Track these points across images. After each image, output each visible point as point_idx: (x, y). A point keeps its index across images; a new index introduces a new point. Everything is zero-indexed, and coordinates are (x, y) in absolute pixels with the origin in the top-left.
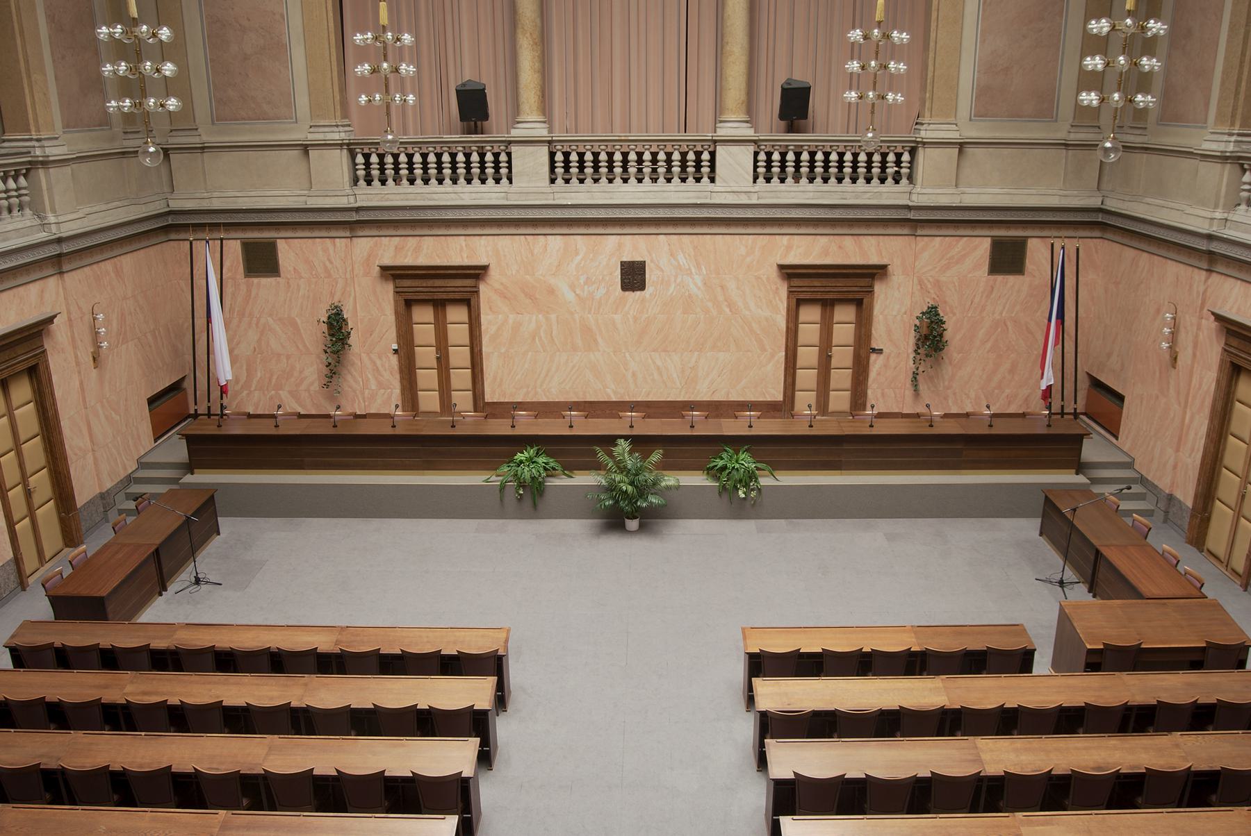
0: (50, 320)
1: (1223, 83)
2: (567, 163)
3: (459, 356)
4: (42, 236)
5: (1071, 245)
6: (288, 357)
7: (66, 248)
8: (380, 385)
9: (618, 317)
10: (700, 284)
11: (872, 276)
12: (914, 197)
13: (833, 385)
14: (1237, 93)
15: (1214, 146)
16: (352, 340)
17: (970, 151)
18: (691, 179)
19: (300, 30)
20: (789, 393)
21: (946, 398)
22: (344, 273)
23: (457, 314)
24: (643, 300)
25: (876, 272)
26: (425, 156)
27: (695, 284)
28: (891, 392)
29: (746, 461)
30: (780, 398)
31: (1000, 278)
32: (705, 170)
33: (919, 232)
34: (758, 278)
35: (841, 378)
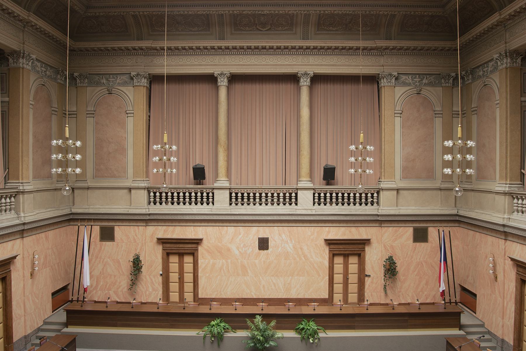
0: (15, 257)
1: (500, 164)
2: (236, 197)
3: (188, 277)
4: (17, 222)
5: (447, 230)
6: (115, 276)
7: (26, 227)
8: (154, 289)
9: (257, 261)
10: (292, 247)
11: (364, 244)
12: (380, 211)
13: (350, 291)
14: (506, 168)
15: (500, 189)
16: (143, 270)
17: (401, 192)
18: (287, 204)
19: (132, 143)
20: (331, 295)
21: (399, 296)
22: (142, 241)
23: (188, 259)
24: (268, 254)
25: (366, 242)
26: (178, 193)
27: (290, 248)
28: (375, 294)
29: (313, 325)
30: (327, 297)
31: (418, 244)
32: (293, 200)
33: (383, 225)
35: (353, 288)
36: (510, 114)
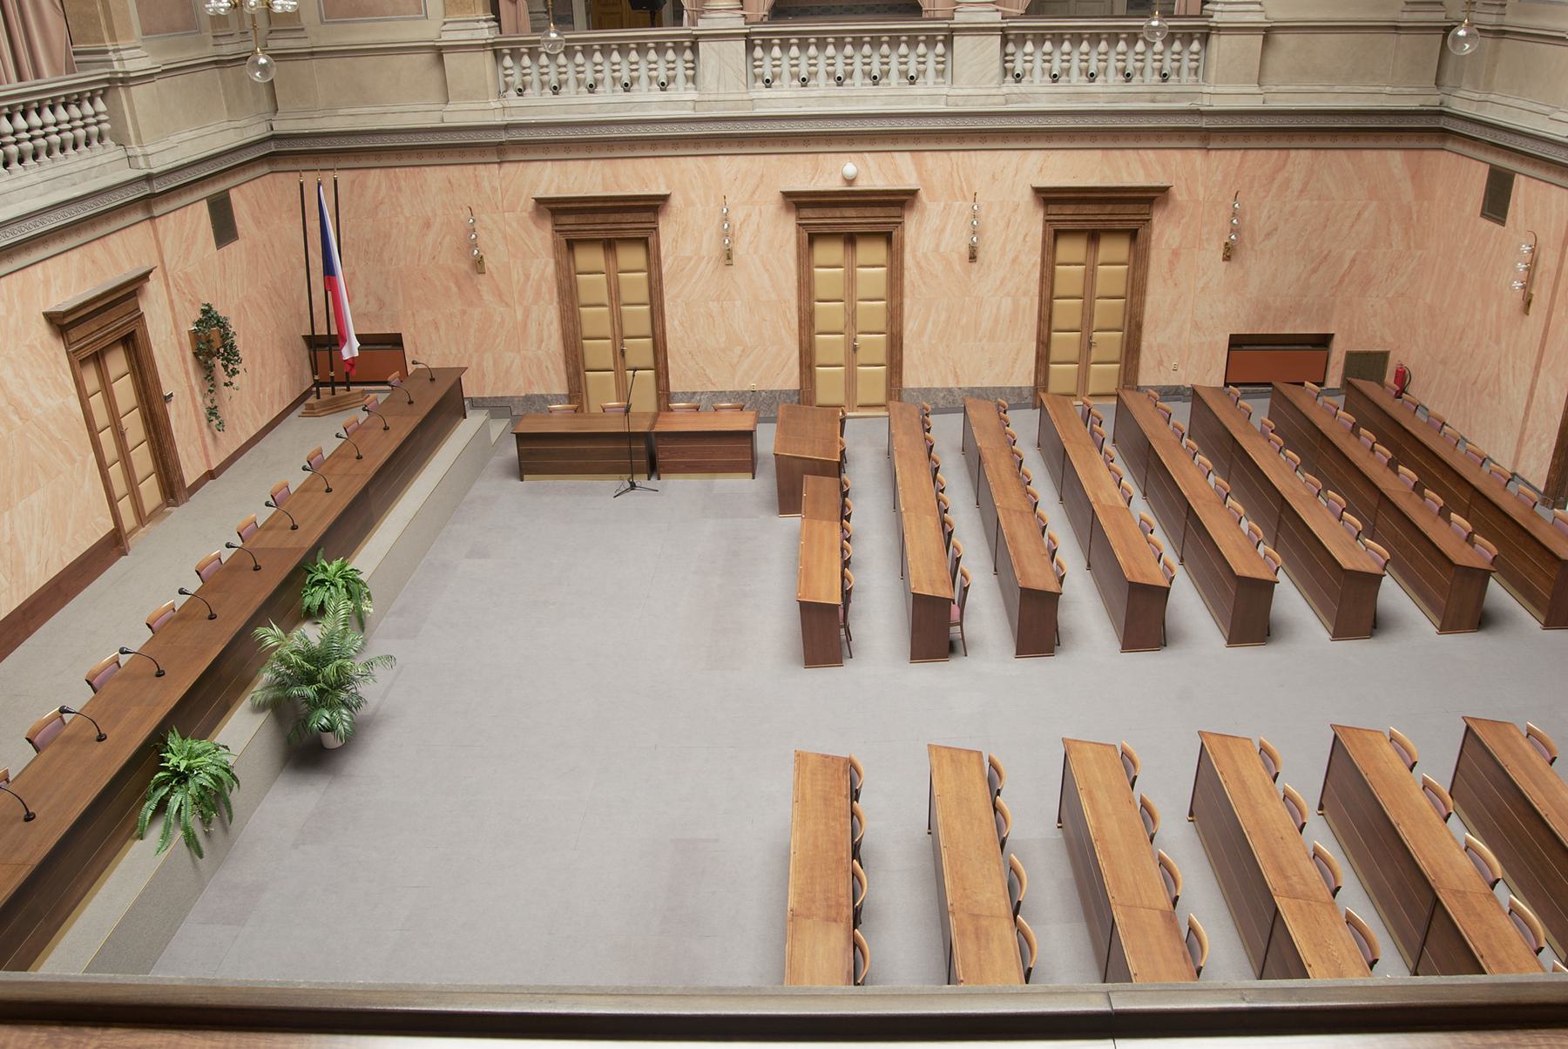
5: (328, 178)
34: (31, 347)
35: (142, 458)
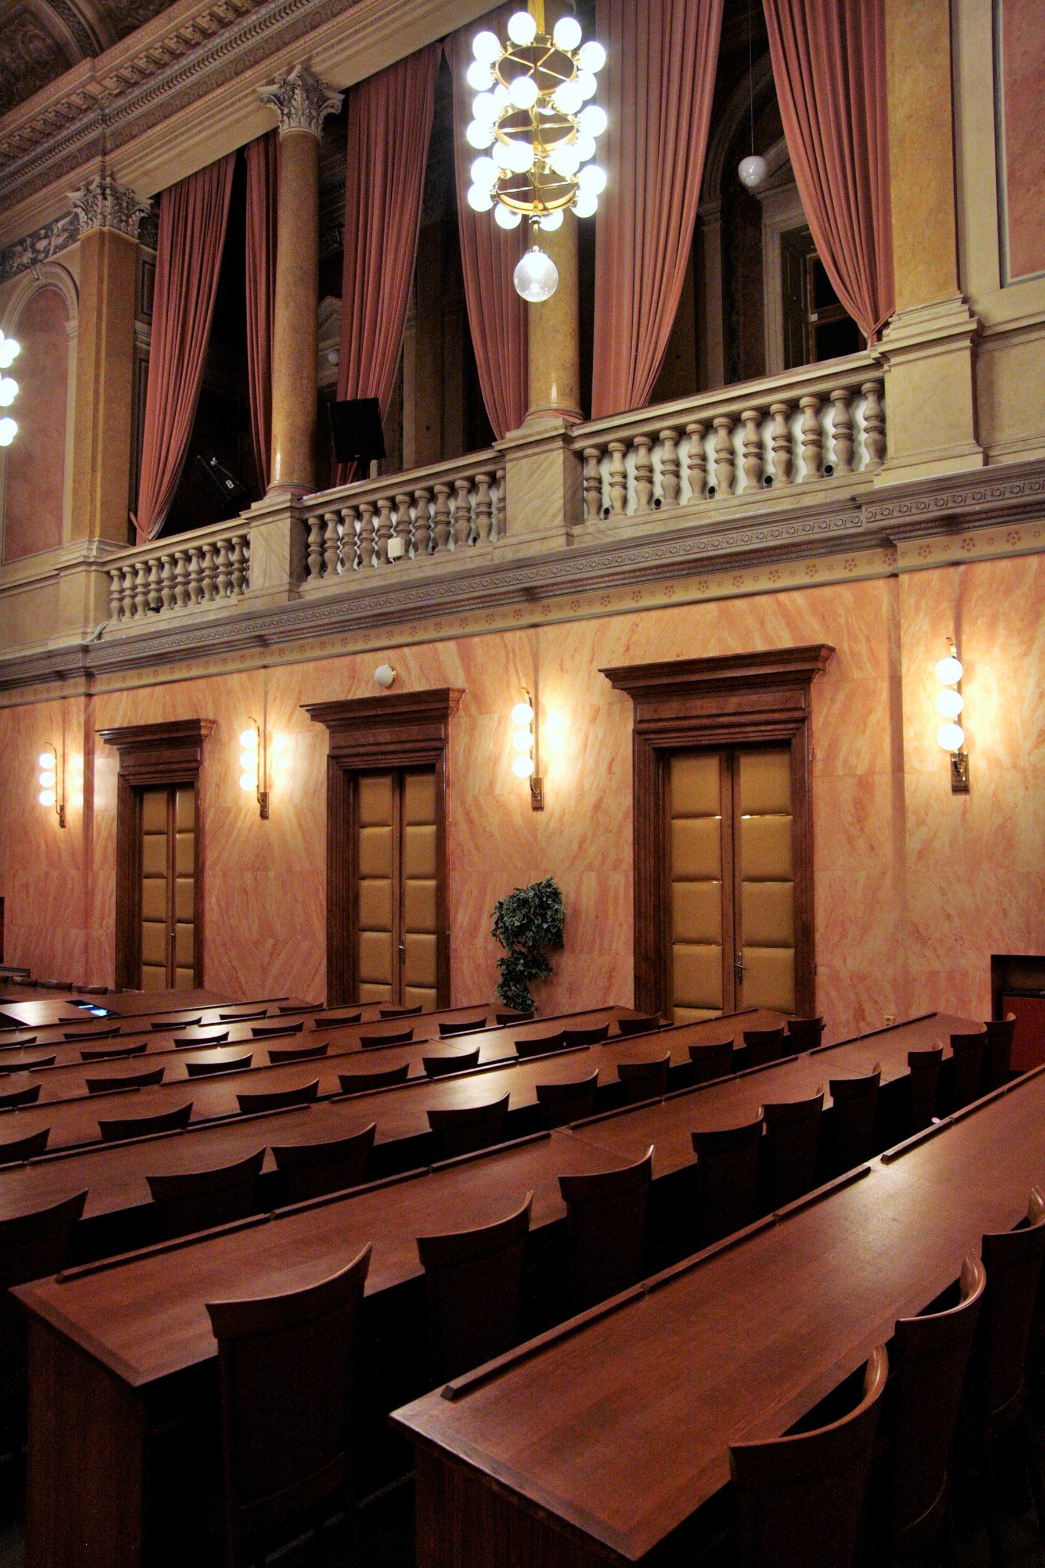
1: (75, 492)
14: (93, 500)
36: (108, 355)
